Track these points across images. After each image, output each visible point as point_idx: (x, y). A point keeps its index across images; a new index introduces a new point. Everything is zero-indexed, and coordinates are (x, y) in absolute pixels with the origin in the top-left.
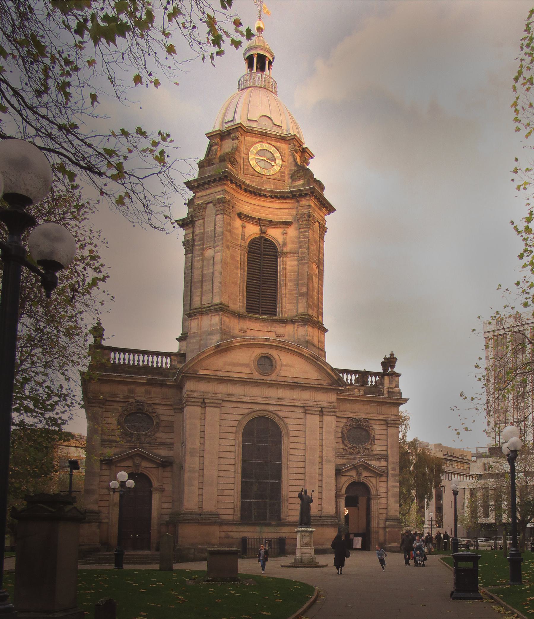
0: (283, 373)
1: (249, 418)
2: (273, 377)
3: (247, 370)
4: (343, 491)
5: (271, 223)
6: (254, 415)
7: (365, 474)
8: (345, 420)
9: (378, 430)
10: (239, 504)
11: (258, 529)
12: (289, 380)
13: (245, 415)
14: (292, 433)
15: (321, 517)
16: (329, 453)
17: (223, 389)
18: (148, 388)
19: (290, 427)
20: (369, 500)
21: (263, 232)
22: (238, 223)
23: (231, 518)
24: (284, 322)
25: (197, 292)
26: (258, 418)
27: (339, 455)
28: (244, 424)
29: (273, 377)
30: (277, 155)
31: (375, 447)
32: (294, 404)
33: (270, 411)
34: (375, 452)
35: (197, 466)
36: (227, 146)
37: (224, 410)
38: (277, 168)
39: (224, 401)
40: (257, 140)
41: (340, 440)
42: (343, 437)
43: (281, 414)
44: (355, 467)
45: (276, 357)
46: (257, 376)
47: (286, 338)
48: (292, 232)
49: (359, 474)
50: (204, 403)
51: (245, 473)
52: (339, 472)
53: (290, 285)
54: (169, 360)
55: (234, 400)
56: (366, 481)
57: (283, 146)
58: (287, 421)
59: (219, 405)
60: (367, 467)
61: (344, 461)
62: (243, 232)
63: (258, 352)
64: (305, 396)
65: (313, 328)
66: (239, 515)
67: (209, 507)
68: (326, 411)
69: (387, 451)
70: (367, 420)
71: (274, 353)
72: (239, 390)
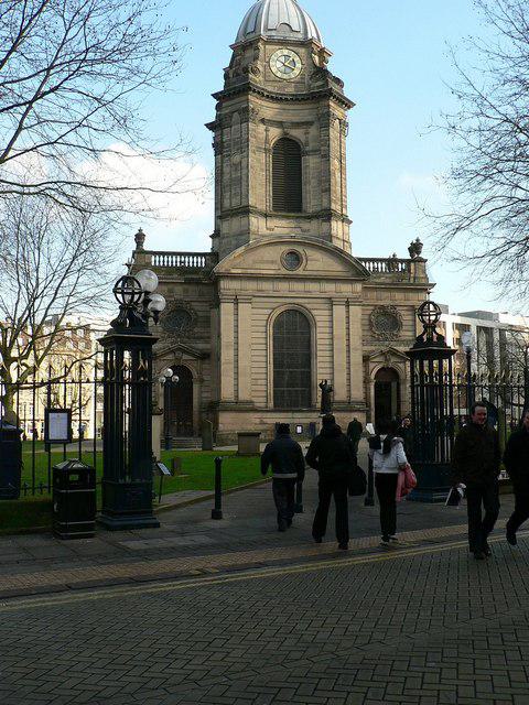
0: (309, 267)
4: (373, 376)
5: (297, 125)
7: (393, 360)
11: (290, 415)
12: (315, 273)
14: (318, 324)
16: (356, 341)
18: (186, 286)
19: (317, 318)
20: (398, 385)
22: (262, 127)
23: (263, 405)
24: (310, 218)
25: (227, 195)
26: (288, 311)
27: (365, 342)
28: (276, 315)
29: (300, 271)
30: (297, 59)
31: (402, 333)
34: (403, 338)
35: (232, 358)
36: (250, 53)
38: (297, 72)
41: (367, 328)
42: (371, 324)
43: (308, 306)
44: (382, 353)
45: (302, 253)
46: (284, 271)
47: (312, 232)
48: (313, 131)
50: (236, 299)
51: (278, 364)
52: (366, 359)
53: (313, 182)
54: (204, 260)
57: (302, 51)
58: (314, 312)
60: (394, 353)
61: (373, 348)
62: (267, 135)
63: (285, 248)
64: (330, 287)
67: (243, 396)
70: (394, 307)
71: (300, 249)
72: (266, 286)
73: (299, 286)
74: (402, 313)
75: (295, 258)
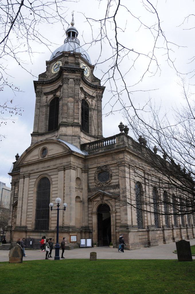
1: (39, 179)
2: (46, 157)
3: (37, 157)
6: (40, 177)
7: (105, 198)
8: (96, 169)
9: (113, 170)
10: (34, 222)
13: (37, 178)
15: (63, 227)
17: (30, 168)
21: (54, 96)
28: (37, 182)
31: (112, 181)
32: (54, 168)
33: (46, 174)
34: (112, 184)
37: (31, 178)
39: (31, 174)
40: (83, 62)
41: (93, 181)
43: (50, 174)
49: (102, 199)
55: (33, 172)
56: (106, 202)
59: (28, 176)
60: (104, 195)
62: (47, 100)
63: (41, 147)
64: (58, 162)
65: (66, 127)
66: (34, 227)
68: (67, 168)
69: (119, 182)
70: (106, 166)
71: (46, 146)
72: (34, 167)
73: (46, 164)
74: (112, 168)
75: (44, 150)
